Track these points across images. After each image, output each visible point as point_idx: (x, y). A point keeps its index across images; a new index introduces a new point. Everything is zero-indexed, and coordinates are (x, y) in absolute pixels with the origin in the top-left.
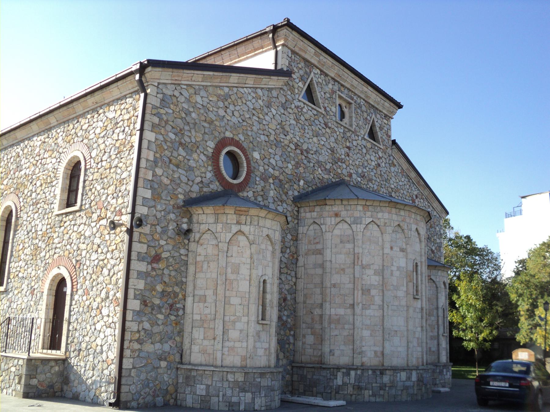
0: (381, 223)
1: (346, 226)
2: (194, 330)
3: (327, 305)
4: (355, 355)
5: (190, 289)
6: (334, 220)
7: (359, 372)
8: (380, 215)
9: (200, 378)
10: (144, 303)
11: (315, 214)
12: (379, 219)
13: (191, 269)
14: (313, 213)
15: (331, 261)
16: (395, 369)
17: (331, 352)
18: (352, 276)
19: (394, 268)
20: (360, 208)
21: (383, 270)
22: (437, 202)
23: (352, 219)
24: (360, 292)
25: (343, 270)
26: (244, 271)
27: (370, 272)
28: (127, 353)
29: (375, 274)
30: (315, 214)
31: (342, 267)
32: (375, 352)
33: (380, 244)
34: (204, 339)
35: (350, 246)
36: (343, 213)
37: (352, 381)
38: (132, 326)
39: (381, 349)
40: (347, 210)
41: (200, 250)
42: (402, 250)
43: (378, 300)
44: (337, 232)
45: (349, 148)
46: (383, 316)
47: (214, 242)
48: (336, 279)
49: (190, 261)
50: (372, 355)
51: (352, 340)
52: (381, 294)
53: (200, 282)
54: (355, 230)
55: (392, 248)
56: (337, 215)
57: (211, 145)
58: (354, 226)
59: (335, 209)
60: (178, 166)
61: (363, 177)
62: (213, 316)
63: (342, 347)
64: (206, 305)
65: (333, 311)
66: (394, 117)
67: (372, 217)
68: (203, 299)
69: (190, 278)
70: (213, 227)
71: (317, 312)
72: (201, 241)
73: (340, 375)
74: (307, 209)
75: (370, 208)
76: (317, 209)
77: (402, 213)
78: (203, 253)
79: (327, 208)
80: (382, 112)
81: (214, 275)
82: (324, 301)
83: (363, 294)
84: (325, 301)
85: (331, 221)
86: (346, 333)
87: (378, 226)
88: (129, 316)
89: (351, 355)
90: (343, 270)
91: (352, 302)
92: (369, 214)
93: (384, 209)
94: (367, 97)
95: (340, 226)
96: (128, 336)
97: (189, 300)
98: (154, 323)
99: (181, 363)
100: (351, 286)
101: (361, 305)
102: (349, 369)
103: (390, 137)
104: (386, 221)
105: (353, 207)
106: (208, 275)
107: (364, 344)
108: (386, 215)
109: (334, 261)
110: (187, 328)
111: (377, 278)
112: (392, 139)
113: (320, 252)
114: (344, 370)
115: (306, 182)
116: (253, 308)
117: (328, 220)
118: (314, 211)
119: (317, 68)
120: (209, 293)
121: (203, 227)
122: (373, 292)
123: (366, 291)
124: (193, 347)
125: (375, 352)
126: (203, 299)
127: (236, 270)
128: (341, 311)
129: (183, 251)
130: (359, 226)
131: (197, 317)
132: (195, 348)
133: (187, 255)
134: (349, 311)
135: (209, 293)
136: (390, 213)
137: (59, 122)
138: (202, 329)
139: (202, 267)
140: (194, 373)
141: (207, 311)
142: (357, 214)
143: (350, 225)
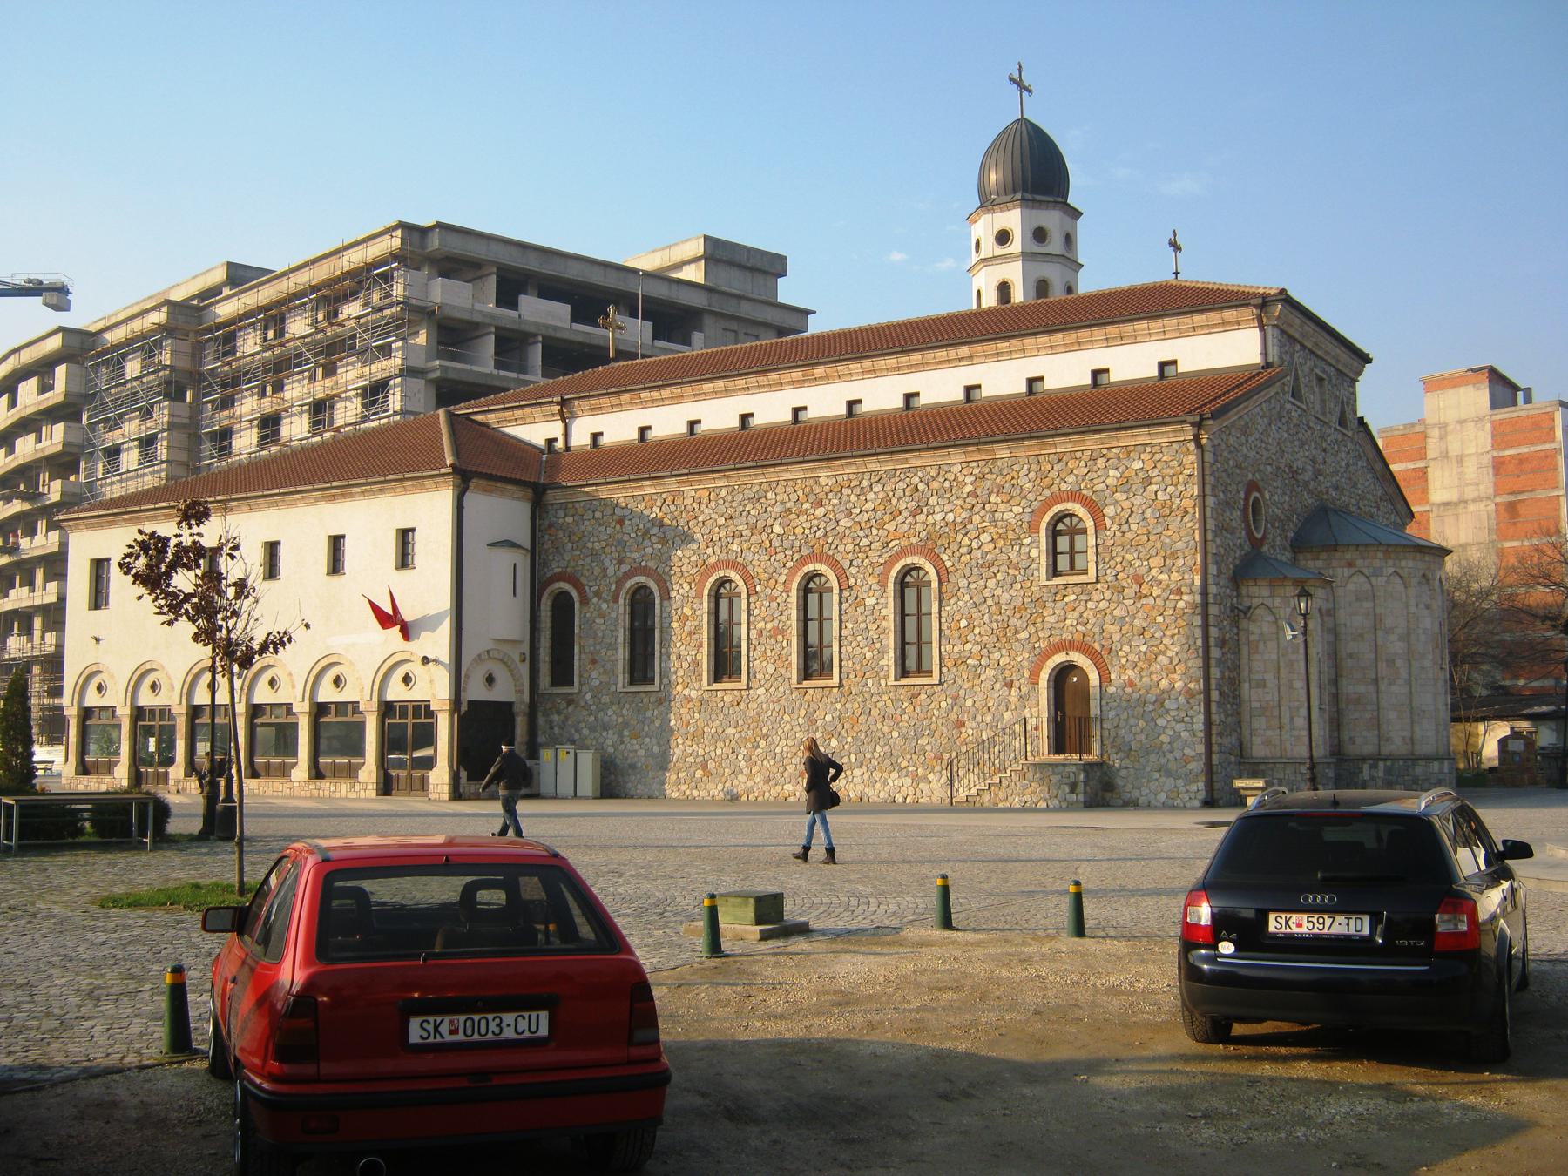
0: (1404, 573)
1: (1362, 579)
2: (1254, 720)
3: (1344, 682)
4: (1382, 743)
5: (1245, 674)
6: (1347, 572)
7: (1389, 763)
8: (1403, 563)
9: (1270, 773)
10: (1221, 694)
11: (1320, 563)
12: (1402, 568)
13: (1244, 651)
14: (1317, 562)
15: (1345, 625)
16: (1428, 759)
17: (1352, 740)
18: (1373, 644)
19: (1420, 631)
20: (1380, 555)
21: (1409, 634)
22: (1402, 502)
23: (1371, 570)
24: (1384, 664)
25: (1361, 636)
27: (1393, 637)
28: (1215, 748)
29: (1399, 640)
30: (1321, 562)
31: (1360, 631)
32: (1404, 738)
33: (1404, 600)
34: (1268, 728)
35: (1368, 605)
36: (1359, 562)
37: (1381, 774)
38: (1215, 718)
39: (1410, 735)
40: (1364, 558)
41: (1252, 627)
42: (1428, 607)
43: (1404, 673)
44: (1351, 586)
45: (1324, 450)
46: (1411, 693)
47: (1271, 618)
49: (1243, 639)
50: (1398, 741)
51: (1377, 723)
52: (1407, 665)
53: (1255, 665)
54: (1374, 583)
55: (1417, 606)
56: (1350, 565)
57: (1242, 495)
58: (1373, 579)
59: (1348, 556)
60: (1226, 530)
61: (1336, 488)
62: (1276, 703)
63: (1364, 733)
64: (1266, 690)
65: (1351, 689)
66: (1360, 378)
67: (1394, 565)
68: (1262, 684)
69: (1244, 661)
70: (1268, 602)
72: (1253, 618)
73: (1366, 767)
74: (1309, 556)
75: (1393, 555)
76: (1324, 556)
77: (1427, 558)
78: (1257, 631)
79: (1338, 555)
80: (1348, 376)
81: (1274, 657)
83: (1388, 666)
84: (1341, 676)
85: (1342, 572)
86: (1368, 716)
87: (1401, 577)
88: (1214, 708)
89: (1376, 742)
90: (1361, 636)
91: (1374, 676)
92: (1390, 562)
93: (1407, 555)
94: (1338, 361)
95: (1355, 578)
96: (1214, 731)
97: (1246, 686)
98: (1227, 715)
99: (1242, 756)
100: (1372, 656)
101: (1386, 680)
102: (1376, 759)
103: (1355, 413)
104: (1411, 571)
105: (1371, 553)
106: (1266, 657)
107: (1390, 728)
108: (1411, 563)
109: (1348, 624)
110: (1246, 717)
111: (1401, 644)
112: (1359, 415)
114: (1371, 762)
115: (1298, 515)
117: (1339, 571)
118: (1318, 559)
119: (1299, 342)
120: (1269, 677)
121: (1256, 602)
122: (1399, 663)
123: (1391, 662)
124: (1254, 738)
125: (1404, 738)
128: (1361, 689)
129: (1235, 631)
130: (1379, 579)
131: (1257, 705)
132: (1257, 740)
133: (1237, 634)
134: (1371, 688)
135: (1269, 677)
136: (1414, 559)
137: (1013, 455)
138: (1263, 719)
139: (1257, 647)
140: (1262, 767)
141: (1268, 697)
142: (1377, 563)
143: (1367, 578)
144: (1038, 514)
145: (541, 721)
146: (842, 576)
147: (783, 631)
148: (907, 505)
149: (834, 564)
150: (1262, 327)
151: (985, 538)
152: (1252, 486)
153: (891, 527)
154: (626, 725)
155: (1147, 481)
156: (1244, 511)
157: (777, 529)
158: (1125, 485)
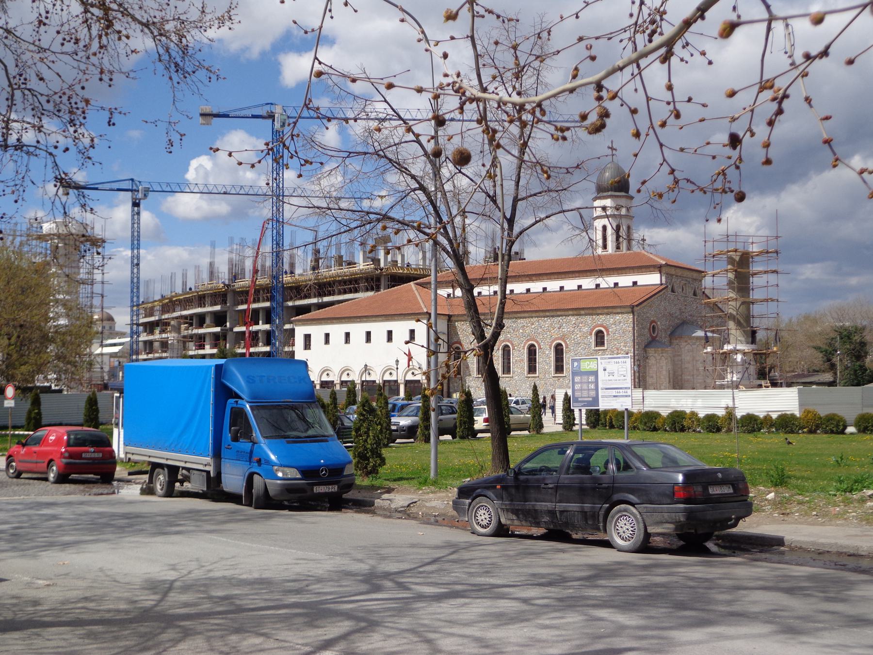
13: (647, 368)
26: (664, 368)
27: (699, 363)
48: (687, 365)
53: (651, 372)
56: (686, 342)
68: (652, 377)
71: (680, 378)
82: (682, 374)
85: (684, 344)
113: (680, 355)
116: (667, 379)
120: (654, 375)
126: (652, 377)
127: (662, 367)
128: (689, 377)
135: (654, 375)
144: (592, 330)
145: (451, 385)
146: (539, 345)
147: (523, 360)
148: (557, 326)
149: (537, 342)
150: (660, 273)
151: (578, 336)
152: (653, 321)
153: (553, 331)
154: (477, 387)
155: (620, 322)
156: (650, 329)
157: (521, 331)
158: (614, 323)
